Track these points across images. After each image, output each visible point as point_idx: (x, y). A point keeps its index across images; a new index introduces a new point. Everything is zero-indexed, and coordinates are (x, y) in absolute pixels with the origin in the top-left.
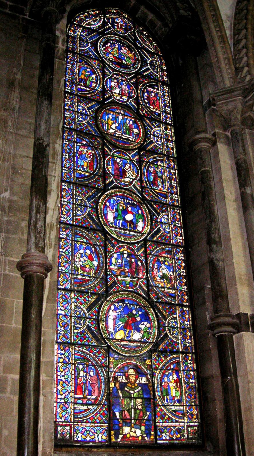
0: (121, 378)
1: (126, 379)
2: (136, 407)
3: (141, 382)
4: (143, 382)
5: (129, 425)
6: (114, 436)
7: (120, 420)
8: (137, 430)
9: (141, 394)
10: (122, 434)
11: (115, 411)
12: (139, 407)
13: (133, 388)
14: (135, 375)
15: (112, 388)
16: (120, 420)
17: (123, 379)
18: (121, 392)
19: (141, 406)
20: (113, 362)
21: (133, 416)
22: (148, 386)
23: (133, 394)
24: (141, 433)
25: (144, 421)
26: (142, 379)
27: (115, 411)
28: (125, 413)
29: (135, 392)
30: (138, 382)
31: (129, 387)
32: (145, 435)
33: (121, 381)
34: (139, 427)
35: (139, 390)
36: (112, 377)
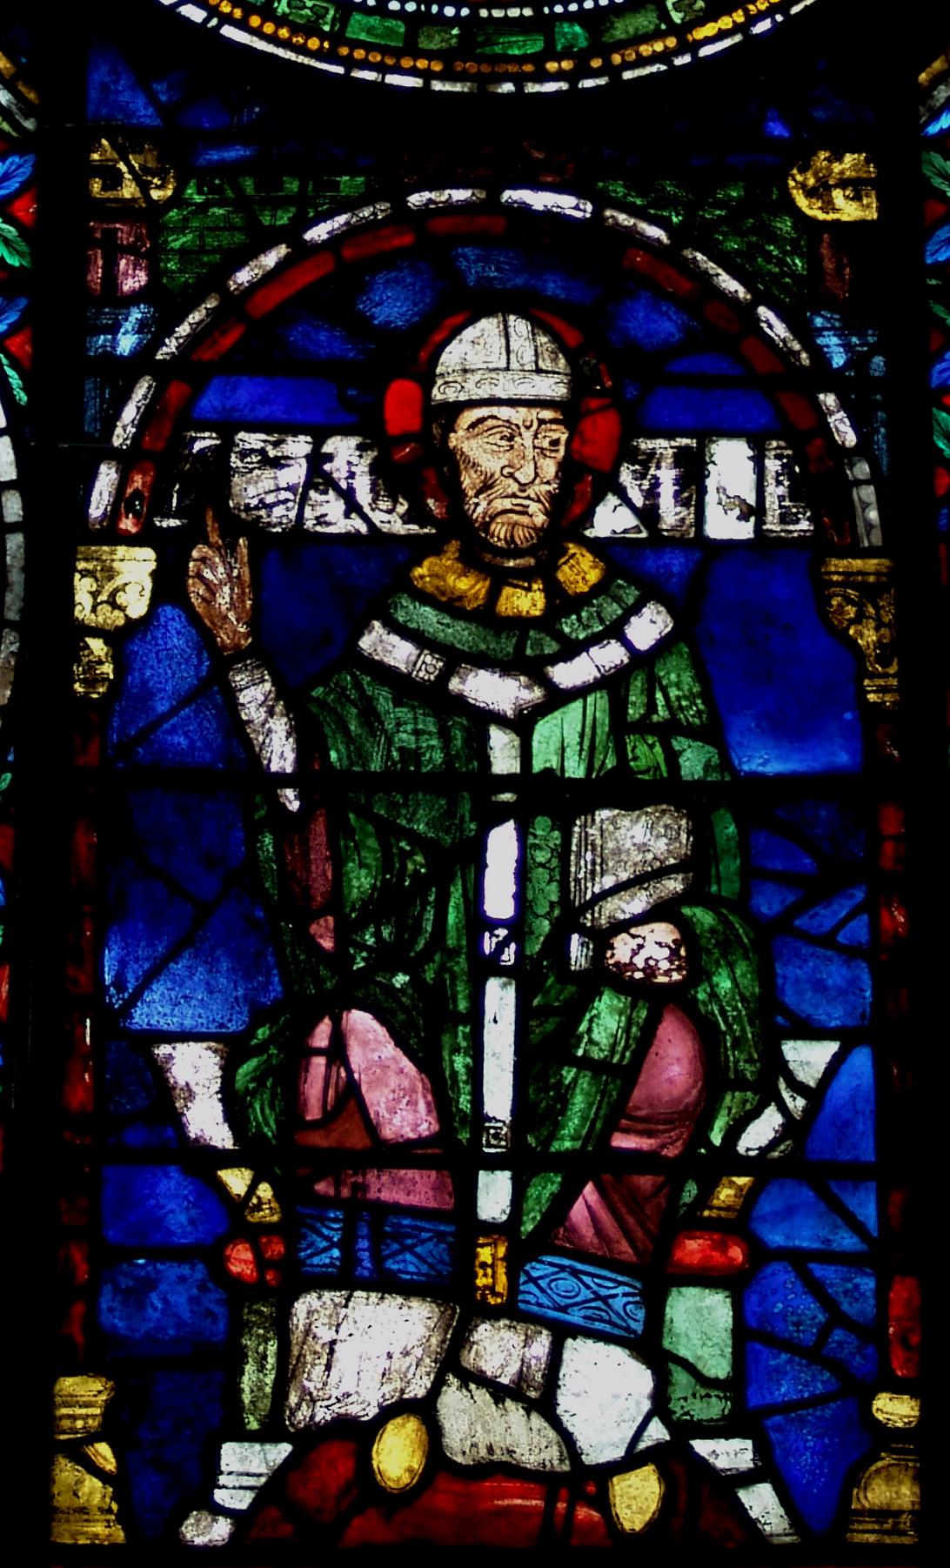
0: (296, 473)
1: (388, 479)
2: (578, 952)
3: (670, 513)
4: (724, 525)
5: (407, 1265)
6: (104, 1453)
7: (236, 1180)
8: (579, 1352)
9: (667, 731)
10: (271, 1432)
11: (141, 1017)
12: (622, 949)
13: (521, 624)
14: (569, 411)
15: (122, 638)
16: (236, 1180)
17: (319, 475)
18: (290, 697)
19: (663, 932)
20: (148, 215)
21: (499, 1100)
22: (821, 587)
23: (522, 724)
24: (660, 1405)
25: (725, 1194)
26: (693, 472)
27: (141, 1017)
28: (337, 1051)
29: (557, 698)
30: (611, 519)
31: (451, 606)
32: (731, 1454)
33: (282, 515)
34: (622, 1296)
35: (641, 661)
36: (127, 461)
